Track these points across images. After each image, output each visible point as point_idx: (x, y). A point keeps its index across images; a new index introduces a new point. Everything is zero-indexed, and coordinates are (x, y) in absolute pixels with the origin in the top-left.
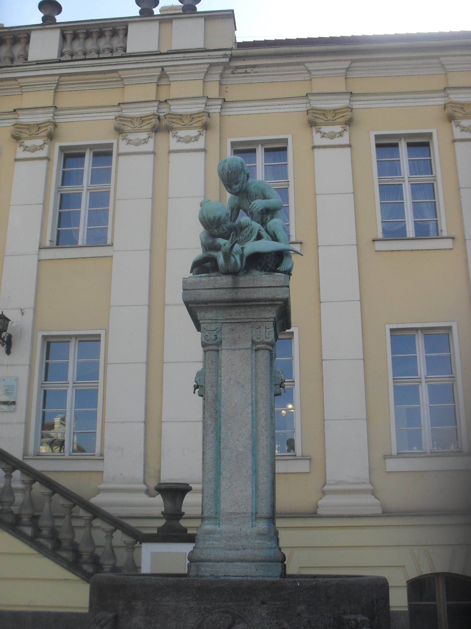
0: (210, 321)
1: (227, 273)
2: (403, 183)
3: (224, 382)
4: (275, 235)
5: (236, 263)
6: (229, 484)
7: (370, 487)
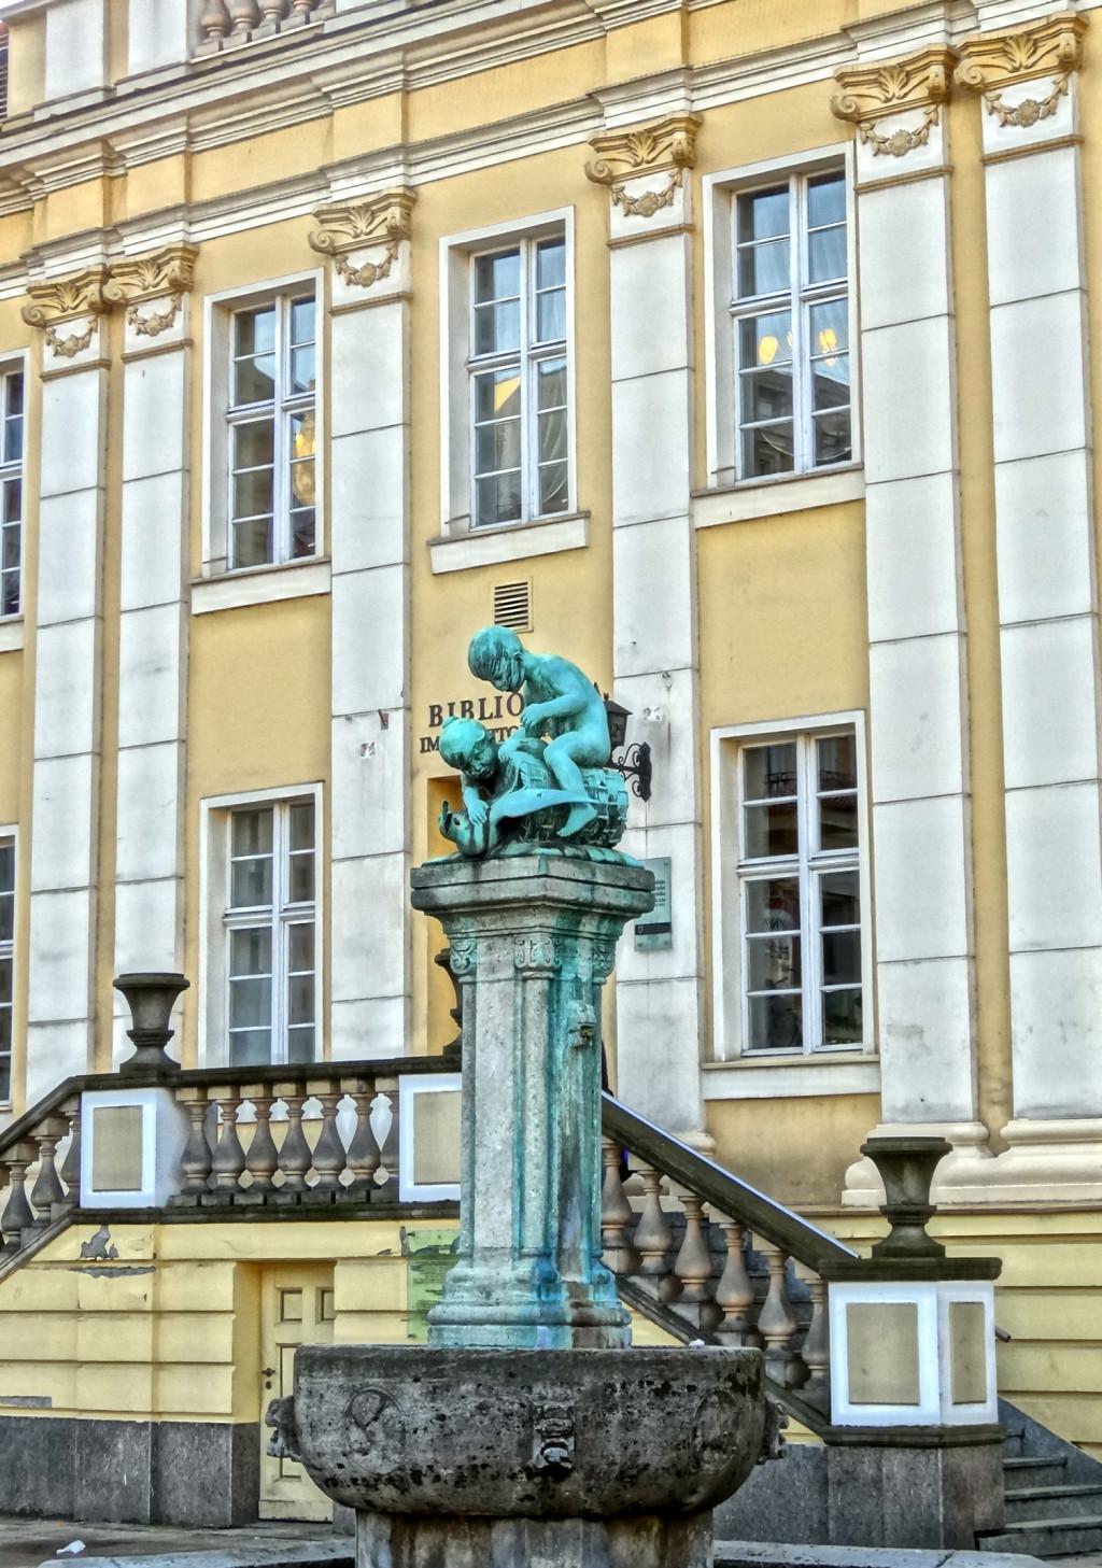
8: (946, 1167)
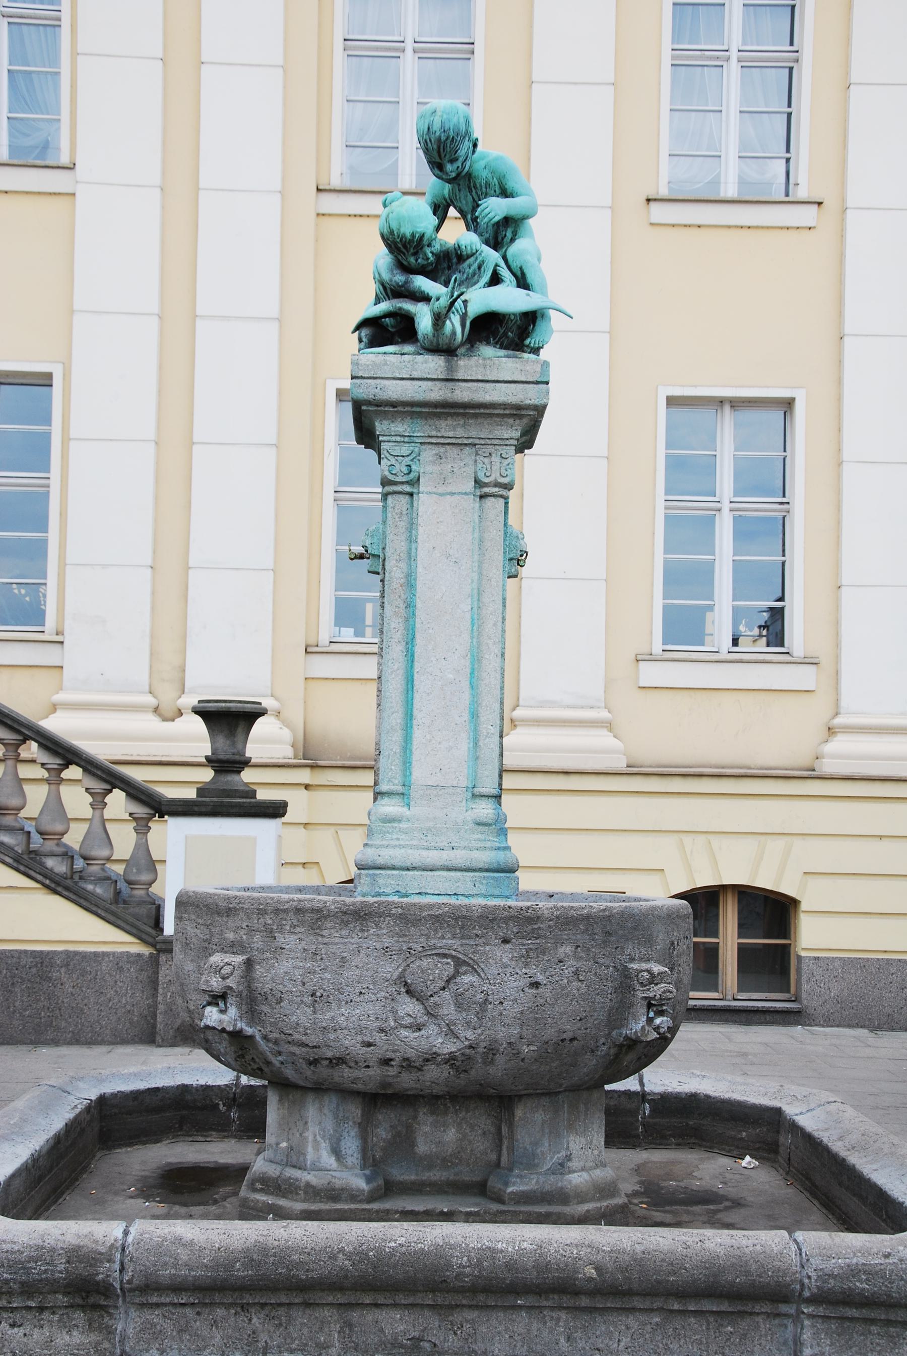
0: (398, 439)
1: (434, 349)
2: (725, 64)
3: (422, 554)
4: (523, 274)
5: (454, 333)
6: (428, 737)
7: (604, 714)
8: (260, 727)
